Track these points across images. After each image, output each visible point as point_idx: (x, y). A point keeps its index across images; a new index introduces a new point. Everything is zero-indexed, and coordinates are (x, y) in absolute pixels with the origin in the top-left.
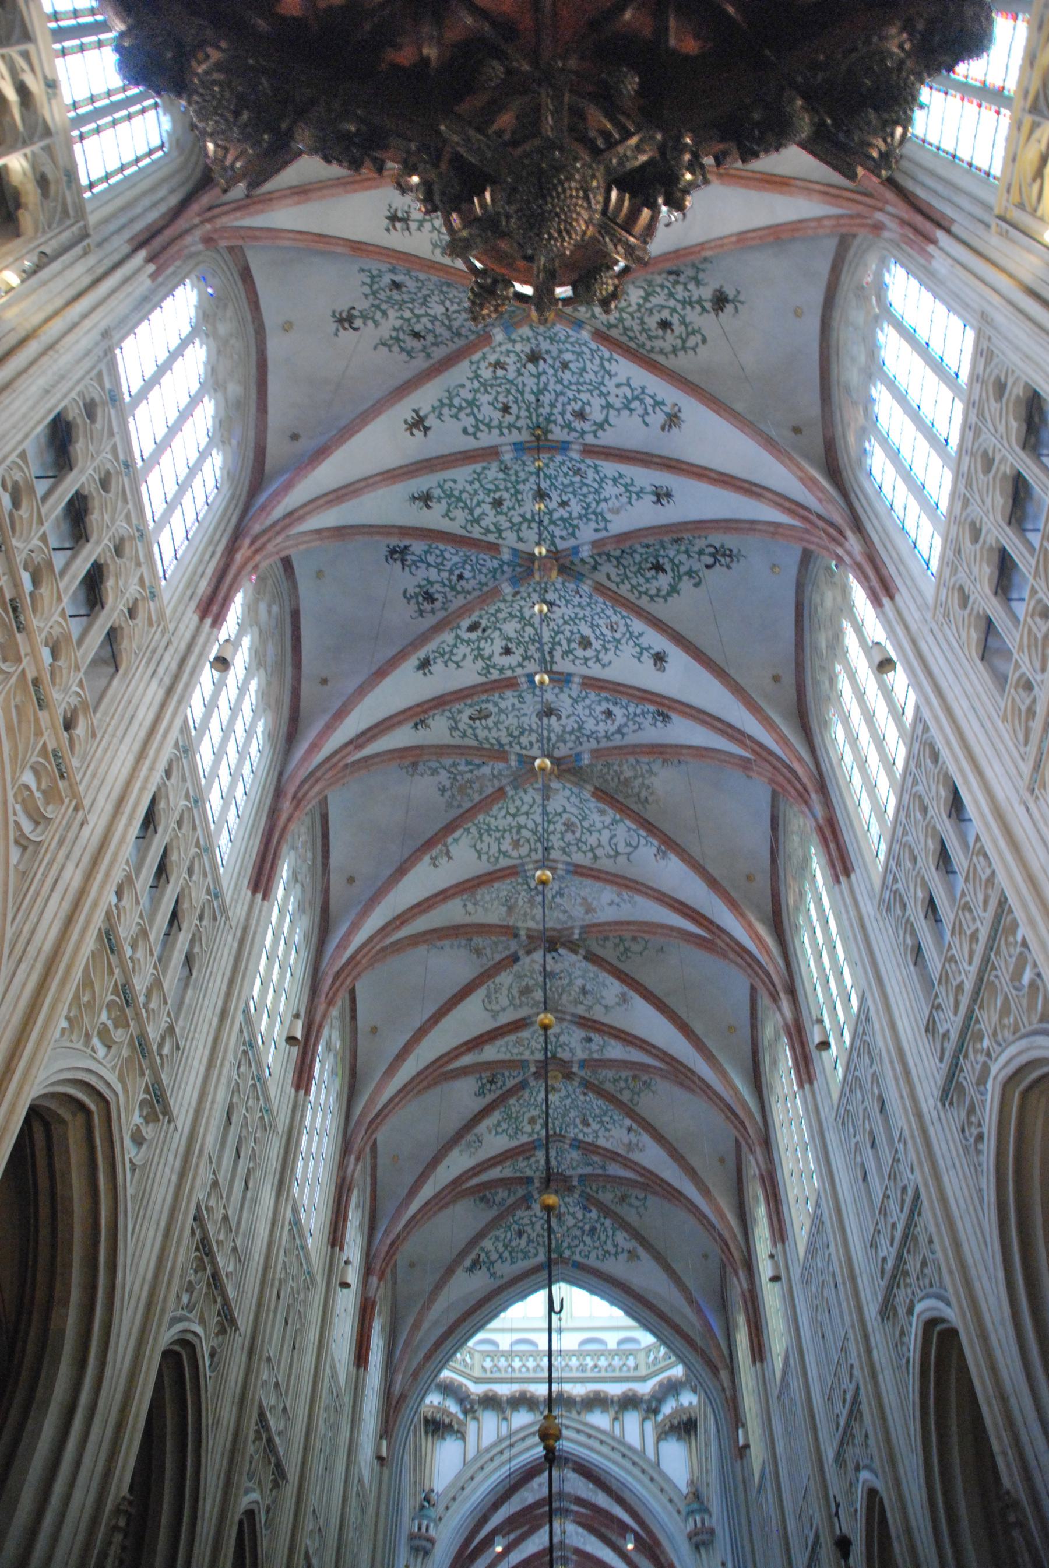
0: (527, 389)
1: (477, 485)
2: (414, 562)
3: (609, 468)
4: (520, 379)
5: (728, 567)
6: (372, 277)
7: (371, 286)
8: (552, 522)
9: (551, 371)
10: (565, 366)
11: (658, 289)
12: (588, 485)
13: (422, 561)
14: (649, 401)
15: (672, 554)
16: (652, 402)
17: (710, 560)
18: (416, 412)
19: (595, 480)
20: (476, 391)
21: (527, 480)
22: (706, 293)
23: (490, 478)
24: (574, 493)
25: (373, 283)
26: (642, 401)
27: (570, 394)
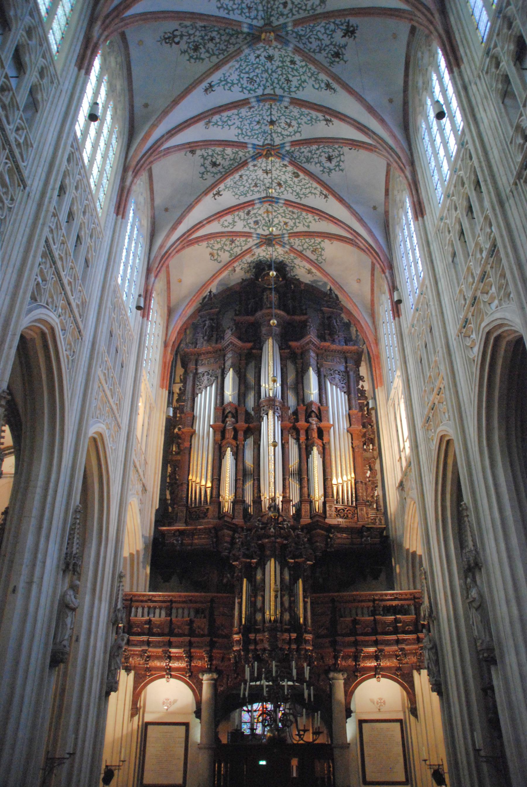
0: (276, 110)
1: (303, 78)
2: (342, 24)
3: (236, 95)
4: (279, 115)
5: (165, 33)
6: (339, 165)
7: (340, 160)
8: (265, 47)
9: (265, 117)
10: (258, 122)
11: (219, 153)
12: (247, 73)
13: (337, 25)
14: (220, 123)
15: (197, 33)
16: (218, 123)
17: (176, 33)
18: (327, 124)
19: (242, 78)
20: (299, 118)
21: (278, 67)
22: (199, 152)
23: (295, 78)
24: (253, 64)
25: (338, 162)
26: (223, 122)
27: (256, 112)
